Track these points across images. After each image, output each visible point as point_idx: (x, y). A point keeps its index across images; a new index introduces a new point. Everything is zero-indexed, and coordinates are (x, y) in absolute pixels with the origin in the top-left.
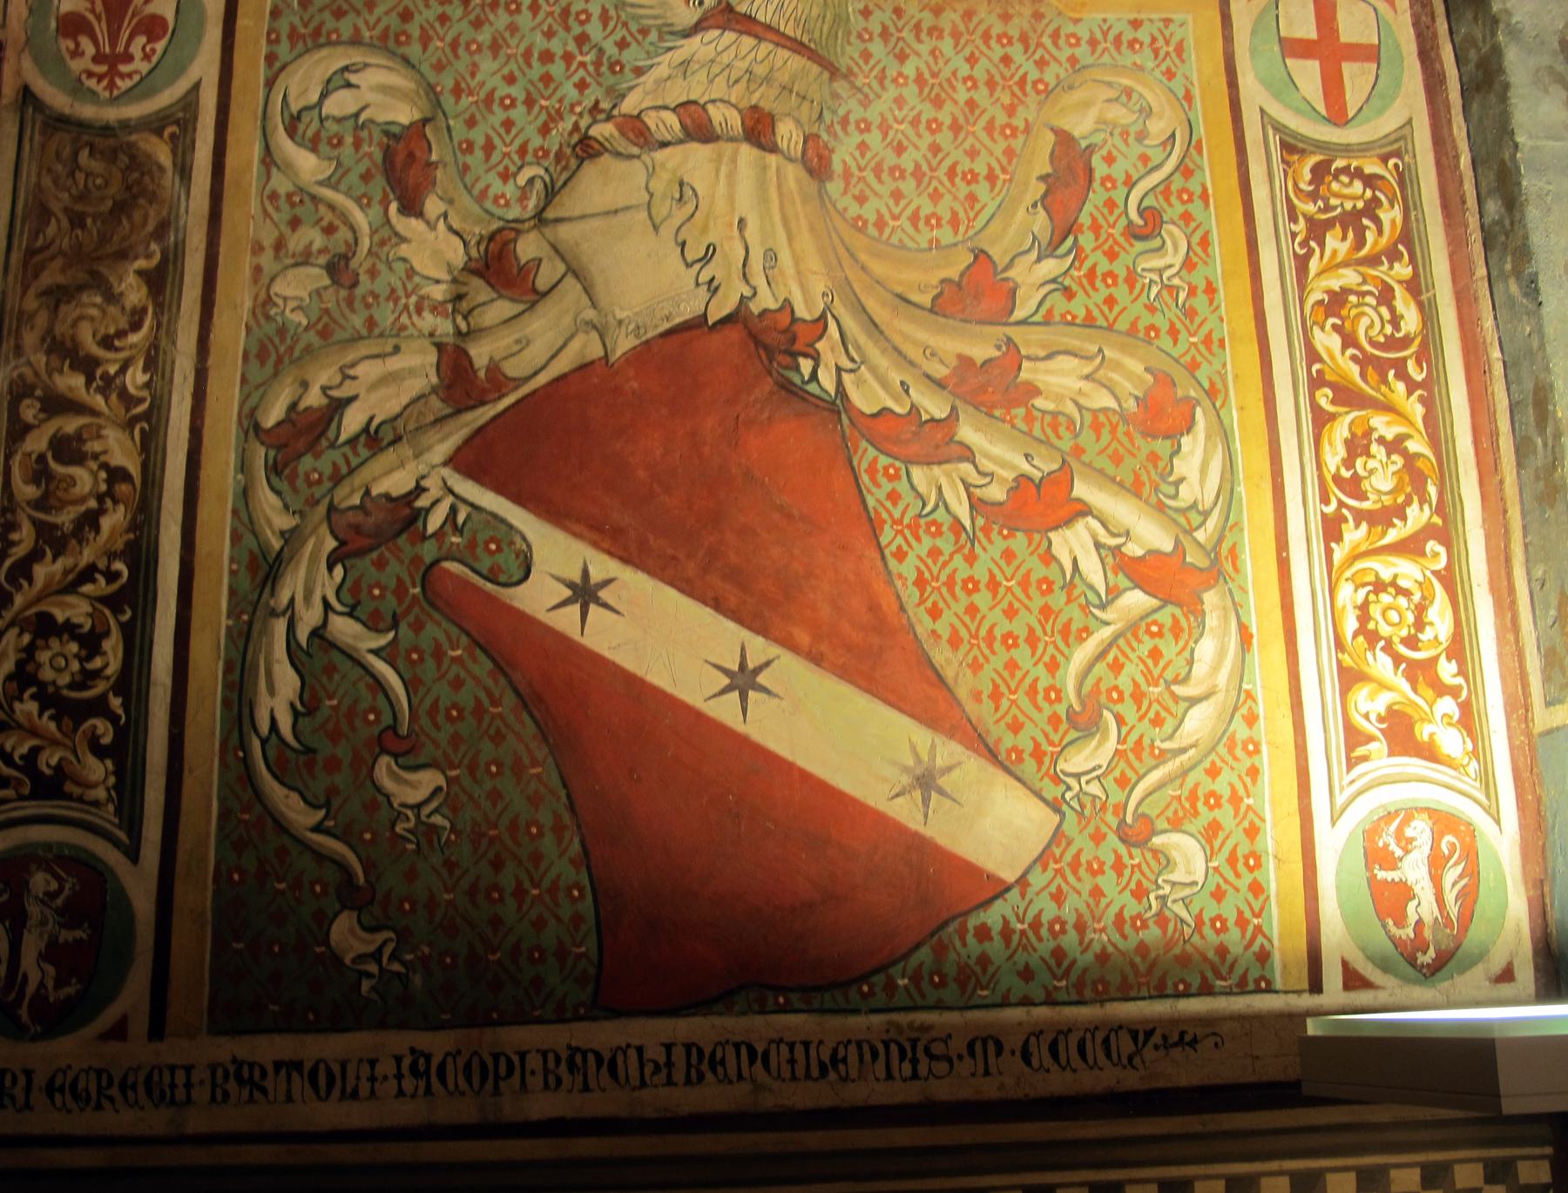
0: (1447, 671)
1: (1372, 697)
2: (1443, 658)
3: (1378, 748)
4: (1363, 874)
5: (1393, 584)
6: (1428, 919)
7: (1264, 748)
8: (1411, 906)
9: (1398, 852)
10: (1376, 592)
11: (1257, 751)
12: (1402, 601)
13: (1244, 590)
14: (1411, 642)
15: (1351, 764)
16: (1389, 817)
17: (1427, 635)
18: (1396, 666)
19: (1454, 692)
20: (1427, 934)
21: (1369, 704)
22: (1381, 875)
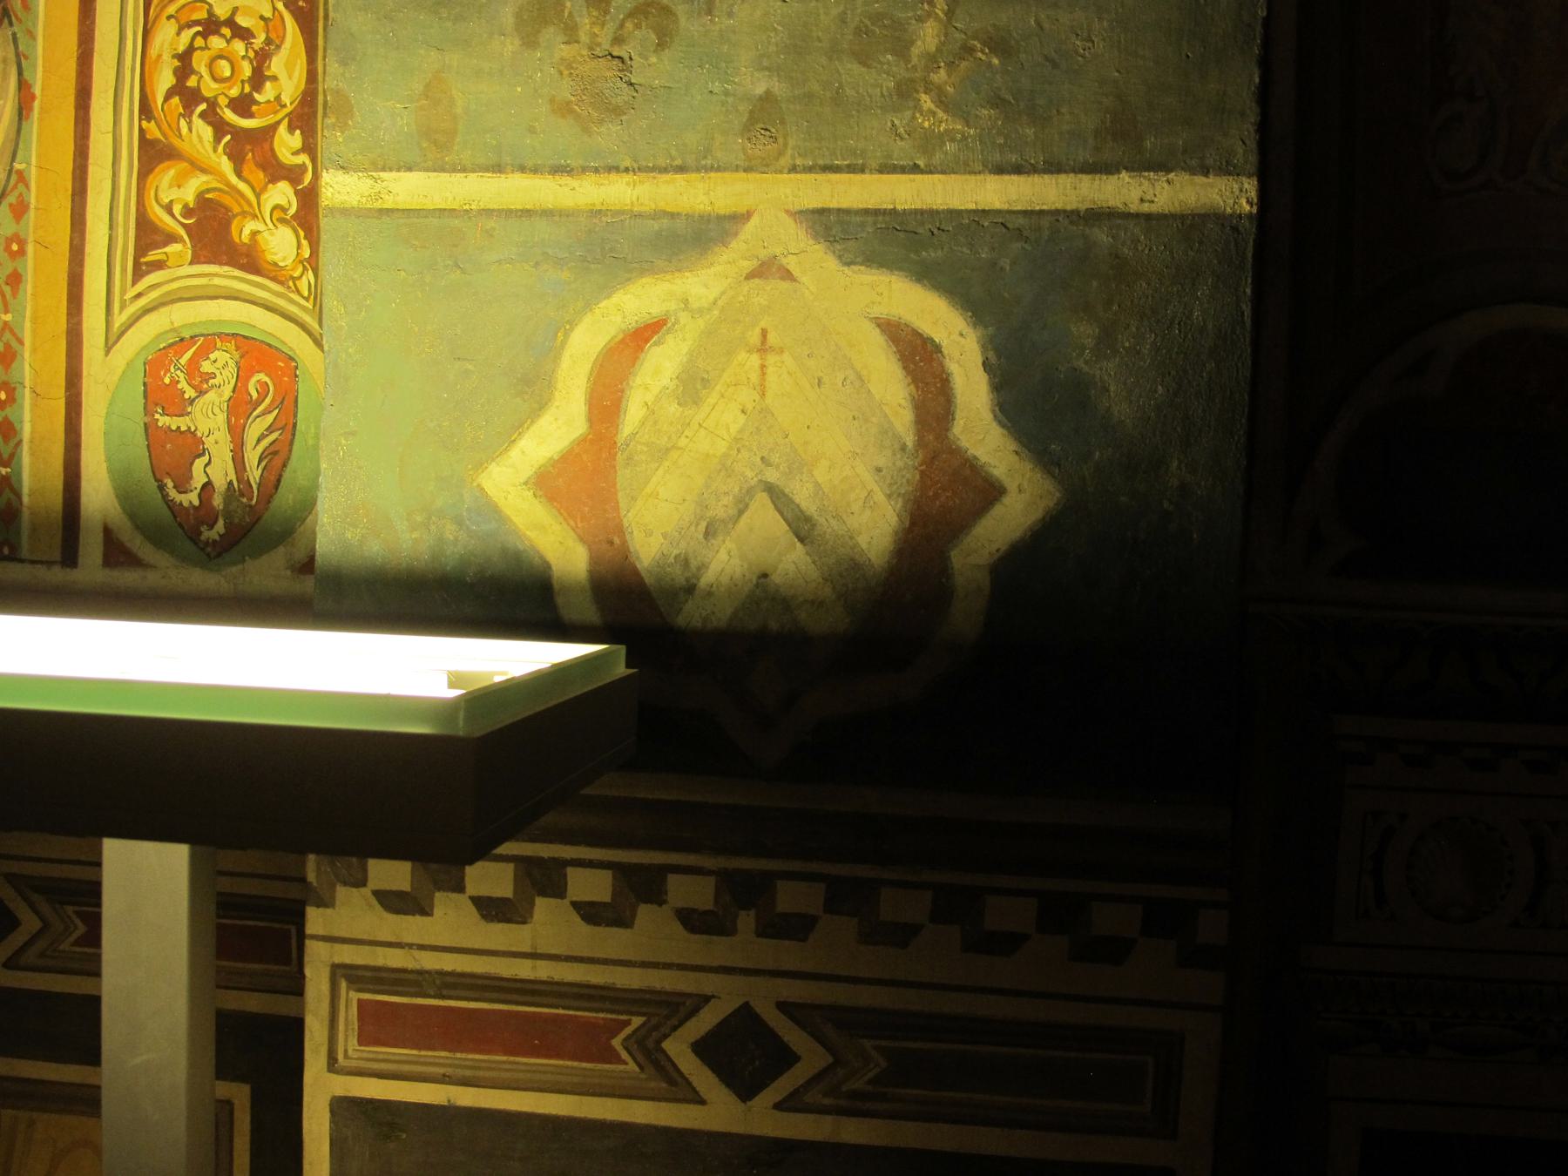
0: (287, 144)
1: (178, 183)
2: (282, 129)
3: (179, 250)
4: (140, 418)
5: (230, 22)
6: (220, 483)
7: (30, 248)
8: (199, 464)
9: (190, 393)
10: (205, 35)
11: (22, 252)
12: (239, 47)
13: (31, 35)
14: (243, 105)
15: (138, 274)
16: (182, 343)
17: (267, 93)
18: (217, 139)
19: (292, 175)
20: (217, 501)
21: (176, 191)
22: (163, 421)
